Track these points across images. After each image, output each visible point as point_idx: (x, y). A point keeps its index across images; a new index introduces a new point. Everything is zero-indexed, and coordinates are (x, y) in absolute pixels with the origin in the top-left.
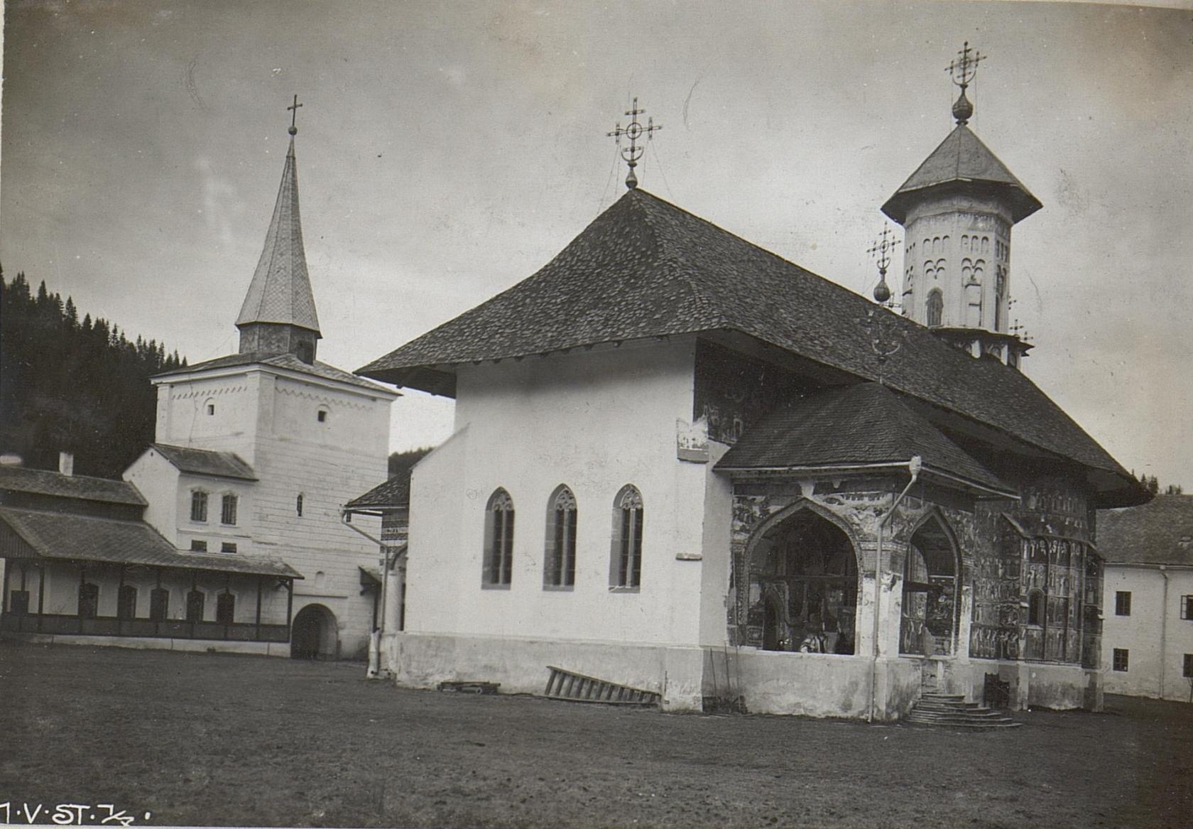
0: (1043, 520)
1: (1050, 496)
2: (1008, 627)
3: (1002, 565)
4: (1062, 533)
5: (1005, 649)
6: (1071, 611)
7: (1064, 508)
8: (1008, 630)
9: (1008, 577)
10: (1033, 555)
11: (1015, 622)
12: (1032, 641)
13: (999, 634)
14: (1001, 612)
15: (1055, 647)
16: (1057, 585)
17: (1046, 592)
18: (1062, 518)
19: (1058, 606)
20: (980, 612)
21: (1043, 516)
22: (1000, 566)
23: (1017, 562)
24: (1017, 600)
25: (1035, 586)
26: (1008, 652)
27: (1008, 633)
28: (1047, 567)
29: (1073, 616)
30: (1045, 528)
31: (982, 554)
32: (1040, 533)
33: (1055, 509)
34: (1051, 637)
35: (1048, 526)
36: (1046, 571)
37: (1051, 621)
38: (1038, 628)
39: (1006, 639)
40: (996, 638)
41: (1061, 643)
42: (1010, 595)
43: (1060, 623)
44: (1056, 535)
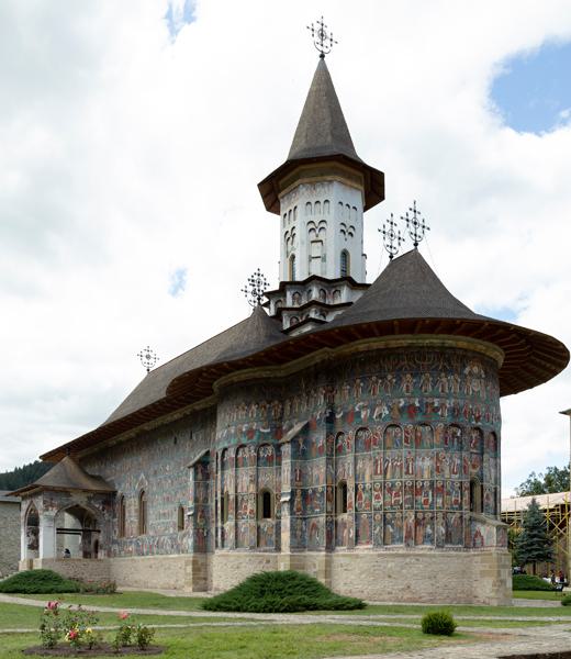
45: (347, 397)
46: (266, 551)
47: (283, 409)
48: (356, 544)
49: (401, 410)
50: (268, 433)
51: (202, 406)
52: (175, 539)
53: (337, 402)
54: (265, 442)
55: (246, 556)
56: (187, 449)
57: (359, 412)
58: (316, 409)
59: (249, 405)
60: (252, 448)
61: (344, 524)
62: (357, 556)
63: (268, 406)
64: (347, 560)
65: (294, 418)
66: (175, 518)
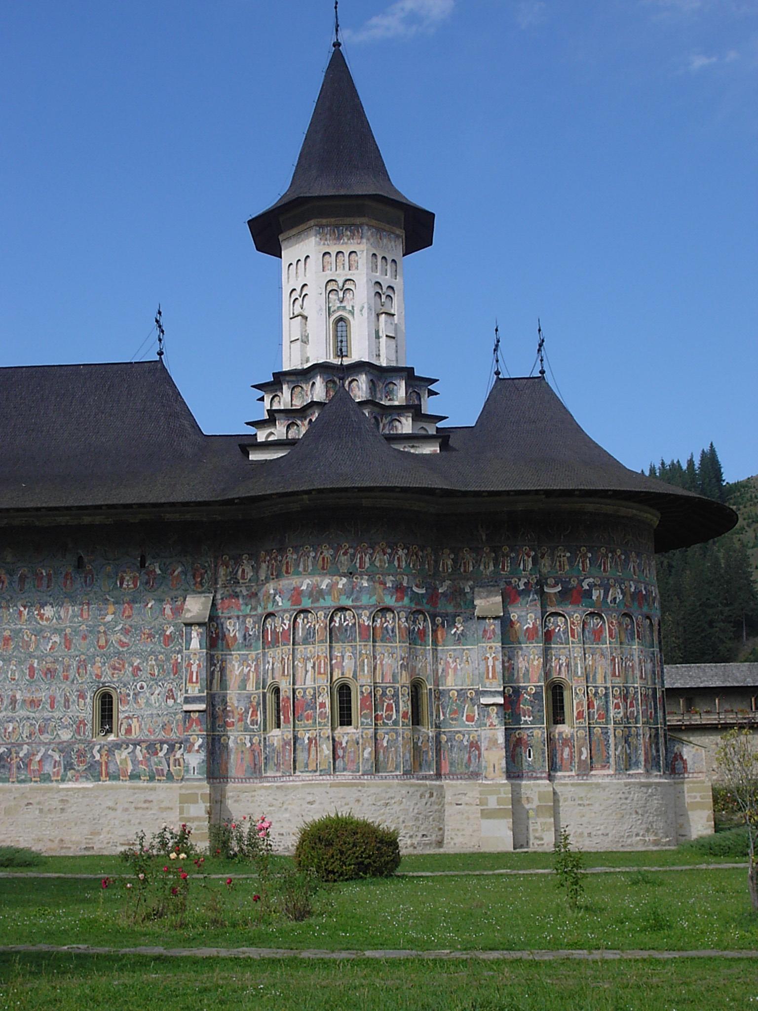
0: (272, 591)
6: (322, 705)
7: (301, 569)
10: (269, 639)
20: (135, 723)
21: (272, 586)
25: (273, 678)
30: (274, 601)
32: (270, 609)
44: (288, 605)
45: (567, 567)
46: (425, 778)
47: (437, 562)
48: (592, 769)
49: (633, 595)
50: (422, 594)
52: (81, 755)
53: (545, 570)
54: (418, 608)
55: (398, 785)
56: (128, 584)
57: (588, 594)
58: (514, 573)
59: (393, 546)
60: (403, 614)
61: (567, 742)
62: (598, 785)
63: (420, 554)
64: (581, 792)
65: (468, 580)
66: (87, 710)
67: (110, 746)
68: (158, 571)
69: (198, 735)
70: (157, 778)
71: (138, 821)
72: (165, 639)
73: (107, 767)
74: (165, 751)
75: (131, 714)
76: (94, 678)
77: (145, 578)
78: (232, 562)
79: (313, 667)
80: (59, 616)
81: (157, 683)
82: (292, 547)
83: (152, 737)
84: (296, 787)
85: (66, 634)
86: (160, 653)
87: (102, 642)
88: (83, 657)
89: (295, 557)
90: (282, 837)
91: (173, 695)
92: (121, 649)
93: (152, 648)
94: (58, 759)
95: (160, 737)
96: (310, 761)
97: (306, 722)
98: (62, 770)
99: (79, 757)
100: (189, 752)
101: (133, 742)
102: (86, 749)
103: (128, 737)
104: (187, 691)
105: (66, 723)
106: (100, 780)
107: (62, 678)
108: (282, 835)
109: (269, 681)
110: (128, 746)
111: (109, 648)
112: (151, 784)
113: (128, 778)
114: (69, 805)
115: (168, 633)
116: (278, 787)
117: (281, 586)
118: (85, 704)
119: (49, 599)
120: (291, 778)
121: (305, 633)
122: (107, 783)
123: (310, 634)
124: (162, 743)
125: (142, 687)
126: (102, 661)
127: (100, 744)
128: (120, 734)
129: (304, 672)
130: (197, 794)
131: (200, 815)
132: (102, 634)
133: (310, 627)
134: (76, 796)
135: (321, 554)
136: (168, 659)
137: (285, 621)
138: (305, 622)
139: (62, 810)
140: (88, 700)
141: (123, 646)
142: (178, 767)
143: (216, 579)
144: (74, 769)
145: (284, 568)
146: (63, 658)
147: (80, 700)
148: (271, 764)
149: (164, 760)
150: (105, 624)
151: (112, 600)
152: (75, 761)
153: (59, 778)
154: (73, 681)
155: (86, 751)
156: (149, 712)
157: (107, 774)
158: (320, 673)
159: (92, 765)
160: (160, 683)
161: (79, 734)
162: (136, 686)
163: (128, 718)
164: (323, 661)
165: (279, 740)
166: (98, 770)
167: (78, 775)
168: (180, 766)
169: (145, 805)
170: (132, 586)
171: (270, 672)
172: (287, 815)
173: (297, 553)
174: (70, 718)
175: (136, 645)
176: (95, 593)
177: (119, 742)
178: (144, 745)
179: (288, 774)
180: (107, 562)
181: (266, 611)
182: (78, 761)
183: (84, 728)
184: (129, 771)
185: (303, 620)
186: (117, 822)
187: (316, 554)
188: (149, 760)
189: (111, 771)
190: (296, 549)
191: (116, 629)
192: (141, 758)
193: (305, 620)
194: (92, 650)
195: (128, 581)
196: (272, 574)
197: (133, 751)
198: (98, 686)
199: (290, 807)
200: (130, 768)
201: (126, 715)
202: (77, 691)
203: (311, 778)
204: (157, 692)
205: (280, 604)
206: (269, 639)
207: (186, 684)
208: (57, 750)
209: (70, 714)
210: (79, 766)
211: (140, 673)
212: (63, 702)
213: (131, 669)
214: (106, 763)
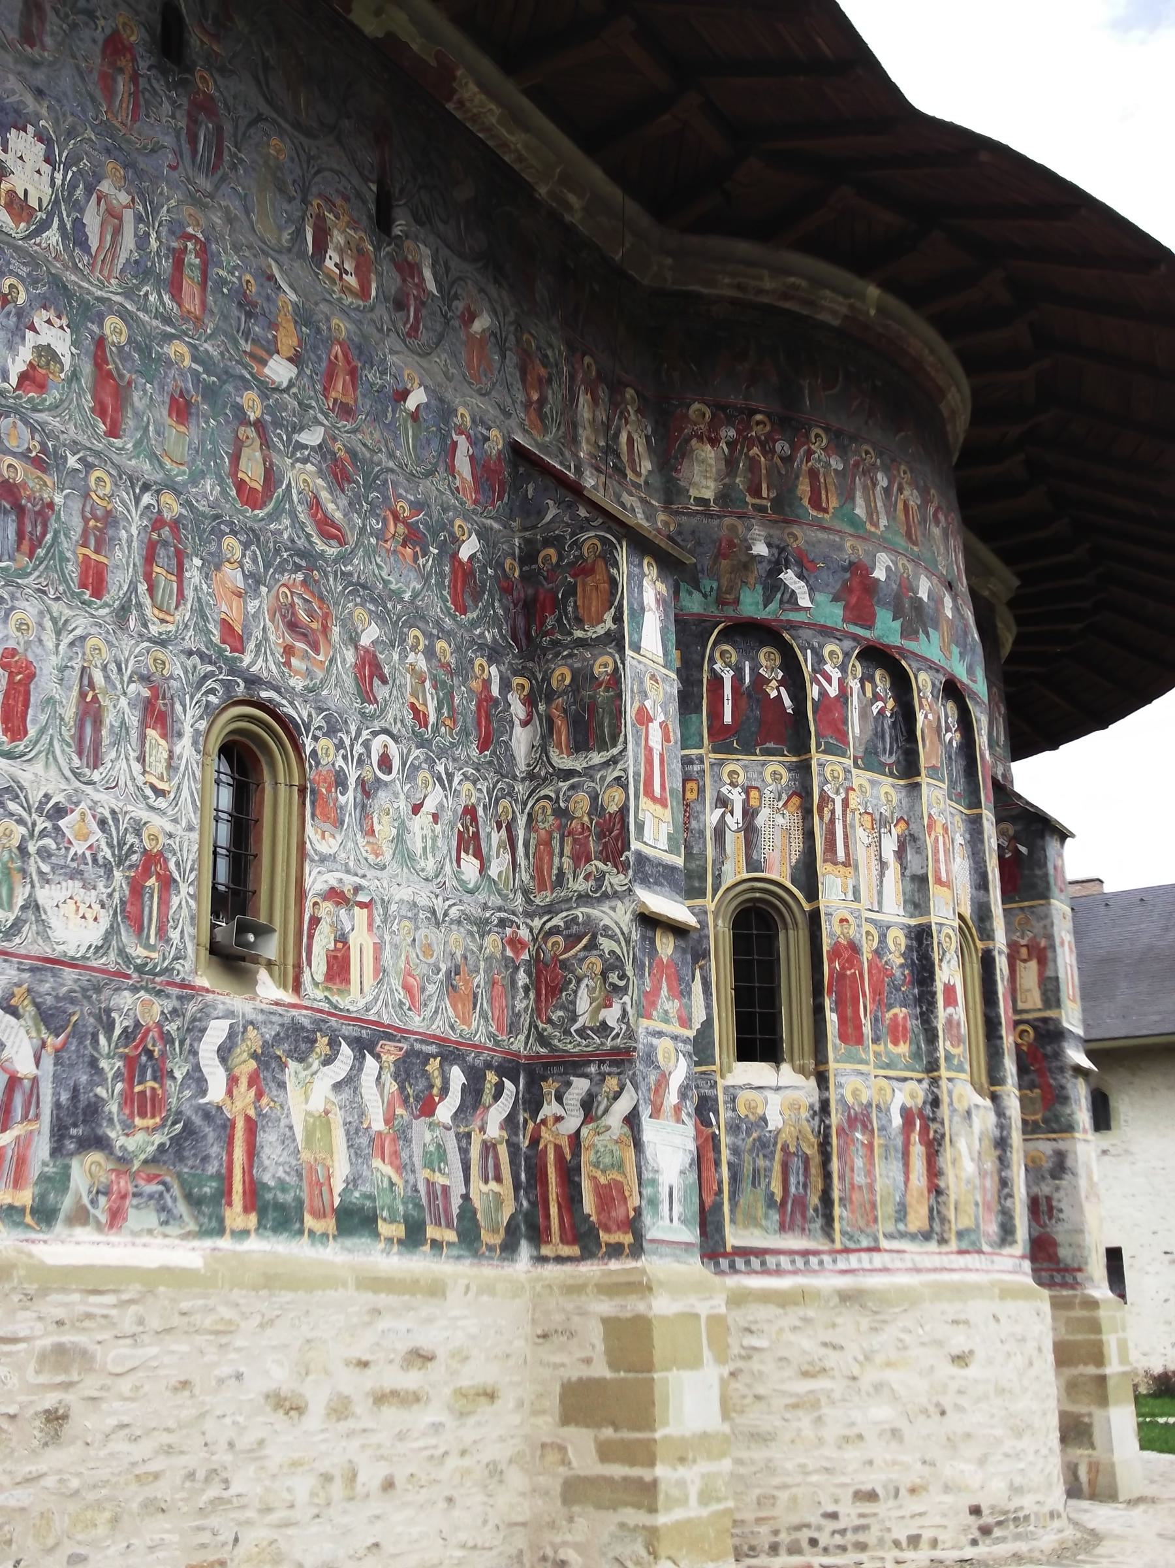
0: (761, 549)
1: (783, 447)
2: (572, 1046)
3: (530, 702)
4: (862, 615)
5: (570, 1174)
8: (574, 1065)
9: (563, 761)
10: (728, 718)
11: (611, 1016)
12: (764, 1146)
13: (532, 1102)
14: (537, 966)
15: (887, 1175)
16: (862, 855)
17: (812, 893)
18: (851, 549)
19: (880, 970)
22: (518, 710)
23: (602, 666)
24: (616, 880)
26: (589, 1204)
27: (580, 1086)
28: (803, 770)
29: (959, 1013)
30: (773, 587)
31: (359, 588)
32: (751, 605)
33: (816, 503)
34: (860, 1119)
35: (789, 577)
36: (803, 792)
37: (851, 1033)
38: (787, 1074)
39: (573, 1121)
40: (510, 1122)
41: (918, 1151)
42: (580, 857)
43: (903, 1049)
44: (833, 614)
51: (516, 140)
67: (269, 1033)
68: (431, 286)
69: (675, 1038)
70: (432, 1232)
71: (381, 1471)
72: (454, 571)
73: (252, 1151)
74: (454, 1099)
75: (350, 881)
76: (216, 639)
77: (394, 282)
78: (603, 392)
79: (900, 854)
80: (79, 225)
81: (431, 762)
82: (827, 430)
83: (416, 1022)
84: (909, 1299)
85: (100, 342)
86: (448, 635)
87: (252, 470)
88: (172, 507)
89: (836, 463)
90: (867, 1508)
91: (476, 835)
92: (319, 545)
93: (415, 595)
94: (25, 1066)
95: (438, 1027)
96: (911, 1199)
97: (890, 1046)
98: (42, 1149)
99: (132, 1070)
100: (656, 1113)
101: (349, 1030)
102: (172, 1027)
103: (335, 999)
104: (640, 827)
105: (79, 848)
106: (220, 1231)
107: (73, 570)
108: (872, 1496)
109: (734, 871)
110: (333, 1044)
111: (273, 517)
112: (420, 1264)
113: (330, 1225)
114: (90, 1385)
115: (464, 554)
116: (846, 1297)
117: (801, 543)
118: (171, 767)
119: (31, 104)
120: (878, 1260)
121: (871, 725)
122: (255, 1245)
123: (883, 737)
124: (450, 1053)
125: (385, 763)
126: (248, 565)
127: (230, 1014)
128: (306, 977)
129: (874, 863)
130: (697, 1316)
131: (709, 1430)
132: (252, 432)
133: (881, 712)
134: (128, 1325)
135: (900, 490)
136: (463, 670)
137: (828, 668)
138: (869, 694)
139: (55, 1418)
140: (185, 747)
141: (326, 536)
142: (493, 1185)
143: (575, 426)
144: (100, 1143)
145: (804, 488)
146: (89, 467)
147: (152, 733)
148: (747, 1195)
149: (452, 1145)
150: (267, 389)
151: (293, 297)
152: (111, 1095)
153: (25, 1197)
154: (122, 614)
155: (167, 1039)
156: (405, 894)
157: (255, 1197)
158: (938, 881)
159: (189, 1131)
160: (440, 768)
161: (139, 928)
162: (367, 745)
163: (335, 895)
164: (941, 839)
165: (794, 1107)
166: (212, 1169)
167: (124, 1184)
168: (498, 1179)
169: (411, 1380)
170: (352, 280)
171: (734, 843)
172: (882, 1413)
173: (843, 452)
174: (102, 823)
175: (370, 554)
176: (230, 220)
177: (303, 1018)
178: (390, 1053)
179: (865, 1243)
180: (275, 116)
181: (730, 612)
182: (127, 1098)
183: (164, 902)
184: (338, 1186)
185: (862, 681)
186: (302, 1486)
187: (890, 483)
188: (402, 1135)
189: (267, 1178)
190: (840, 442)
191: (306, 438)
192: (378, 1124)
193: (868, 686)
194: (208, 484)
195: (341, 251)
196: (757, 493)
197: (350, 1082)
198: (228, 686)
199: (891, 1376)
200: (341, 1169)
201: (332, 879)
202: (145, 679)
203: (938, 1264)
204: (430, 806)
205: (804, 601)
206: (728, 718)
207: (637, 797)
208: (29, 1010)
209: (107, 801)
210: (129, 1129)
211: (382, 692)
212: (70, 711)
213: (350, 656)
214: (252, 1128)
